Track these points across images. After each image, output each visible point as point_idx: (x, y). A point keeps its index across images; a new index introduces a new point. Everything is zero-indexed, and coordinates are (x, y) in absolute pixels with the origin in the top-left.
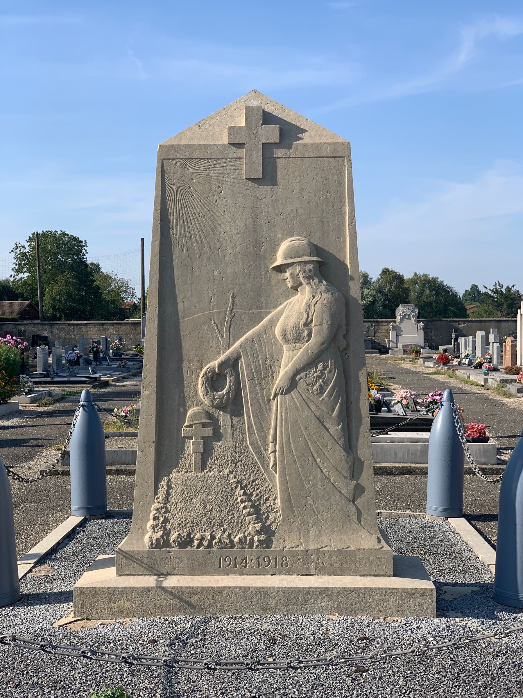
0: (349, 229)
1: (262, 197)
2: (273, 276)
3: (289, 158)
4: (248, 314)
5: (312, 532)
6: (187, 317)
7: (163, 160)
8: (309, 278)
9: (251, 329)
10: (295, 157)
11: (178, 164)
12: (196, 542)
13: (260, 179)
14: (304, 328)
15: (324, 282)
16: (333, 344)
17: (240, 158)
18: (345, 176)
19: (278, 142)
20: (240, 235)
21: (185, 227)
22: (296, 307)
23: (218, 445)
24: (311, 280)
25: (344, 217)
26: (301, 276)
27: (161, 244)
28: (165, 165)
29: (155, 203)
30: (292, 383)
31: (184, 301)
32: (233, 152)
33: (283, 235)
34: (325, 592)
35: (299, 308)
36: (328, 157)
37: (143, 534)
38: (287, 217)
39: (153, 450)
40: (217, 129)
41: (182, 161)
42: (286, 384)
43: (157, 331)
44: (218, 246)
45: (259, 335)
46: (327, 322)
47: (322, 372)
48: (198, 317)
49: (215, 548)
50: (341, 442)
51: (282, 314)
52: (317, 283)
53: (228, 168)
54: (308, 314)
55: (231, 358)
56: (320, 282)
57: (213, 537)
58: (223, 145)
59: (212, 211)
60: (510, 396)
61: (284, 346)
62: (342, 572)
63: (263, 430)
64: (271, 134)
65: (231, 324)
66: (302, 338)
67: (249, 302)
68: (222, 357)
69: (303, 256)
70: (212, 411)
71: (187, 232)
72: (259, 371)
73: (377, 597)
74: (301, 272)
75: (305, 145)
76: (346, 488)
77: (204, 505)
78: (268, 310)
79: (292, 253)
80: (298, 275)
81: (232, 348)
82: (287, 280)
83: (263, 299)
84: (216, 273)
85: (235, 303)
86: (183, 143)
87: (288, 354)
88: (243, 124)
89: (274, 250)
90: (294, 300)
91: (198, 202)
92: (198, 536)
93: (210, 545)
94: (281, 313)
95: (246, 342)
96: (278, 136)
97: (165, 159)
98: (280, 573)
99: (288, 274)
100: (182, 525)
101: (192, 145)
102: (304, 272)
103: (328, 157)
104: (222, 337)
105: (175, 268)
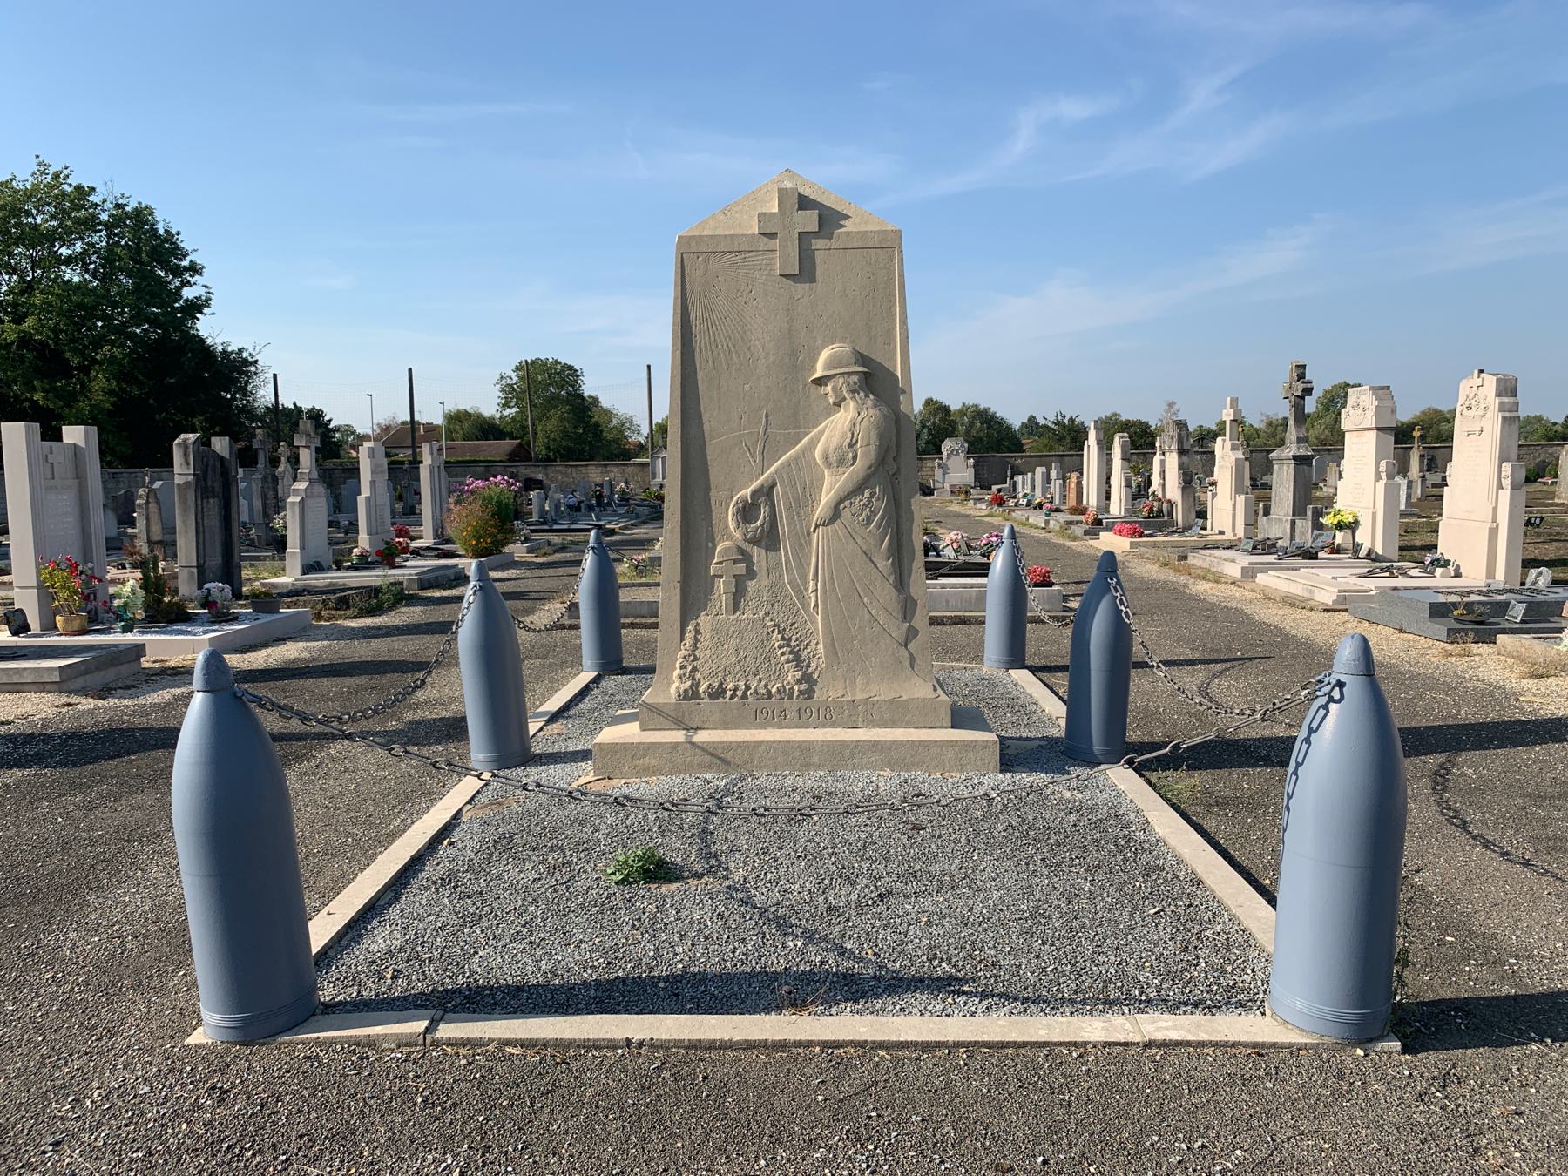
5: (859, 680)
8: (853, 392)
12: (729, 693)
23: (751, 584)
27: (683, 354)
30: (836, 513)
31: (711, 420)
34: (874, 745)
37: (669, 685)
39: (678, 591)
42: (829, 514)
45: (797, 458)
47: (869, 500)
49: (750, 699)
50: (891, 580)
57: (748, 688)
60: (1075, 539)
62: (893, 724)
63: (802, 565)
64: (809, 221)
68: (755, 485)
70: (744, 546)
72: (797, 500)
73: (933, 751)
75: (848, 233)
76: (898, 630)
77: (737, 651)
88: (776, 210)
89: (814, 360)
92: (731, 686)
93: (744, 696)
94: (822, 433)
98: (824, 726)
99: (829, 388)
100: (713, 674)
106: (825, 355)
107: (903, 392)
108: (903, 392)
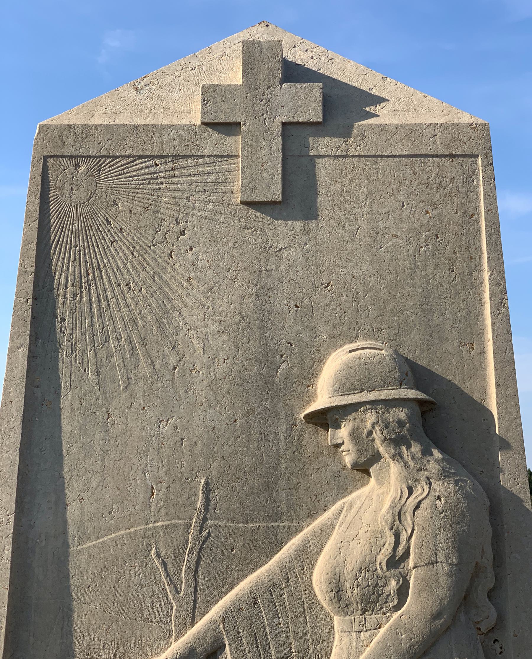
0: (493, 324)
1: (281, 245)
2: (306, 436)
3: (345, 156)
4: (244, 533)
6: (89, 539)
7: (45, 159)
8: (397, 442)
9: (250, 573)
10: (359, 156)
11: (82, 169)
13: (275, 203)
14: (388, 574)
15: (437, 454)
16: (462, 617)
17: (228, 156)
18: (478, 198)
19: (320, 119)
20: (227, 337)
21: (92, 316)
22: (367, 517)
24: (404, 448)
25: (479, 295)
26: (377, 436)
27: (32, 356)
28: (51, 169)
29: (23, 257)
32: (213, 144)
33: (332, 336)
35: (375, 520)
36: (437, 156)
38: (340, 294)
40: (177, 95)
41: (91, 162)
43: (8, 575)
44: (172, 362)
45: (271, 589)
46: (447, 557)
48: (117, 540)
51: (331, 534)
52: (419, 455)
53: (201, 178)
54: (397, 536)
55: (198, 650)
56: (427, 452)
58: (191, 128)
59: (161, 277)
61: (336, 620)
64: (306, 104)
65: (199, 558)
66: (382, 598)
67: (248, 503)
69: (382, 387)
71: (97, 326)
74: (377, 428)
75: (383, 128)
78: (294, 524)
79: (356, 378)
80: (370, 433)
81: (201, 624)
82: (343, 448)
83: (282, 494)
84: (166, 428)
85: (212, 503)
86: (96, 121)
87: (346, 641)
88: (236, 78)
89: (310, 372)
90: (359, 497)
91: (126, 256)
94: (326, 532)
95: (238, 606)
96: (320, 107)
97: (53, 157)
99: (344, 433)
101: (117, 126)
102: (387, 427)
103: (437, 156)
104: (177, 592)
105: (65, 415)
106: (335, 362)
107: (505, 445)
108: (505, 445)
